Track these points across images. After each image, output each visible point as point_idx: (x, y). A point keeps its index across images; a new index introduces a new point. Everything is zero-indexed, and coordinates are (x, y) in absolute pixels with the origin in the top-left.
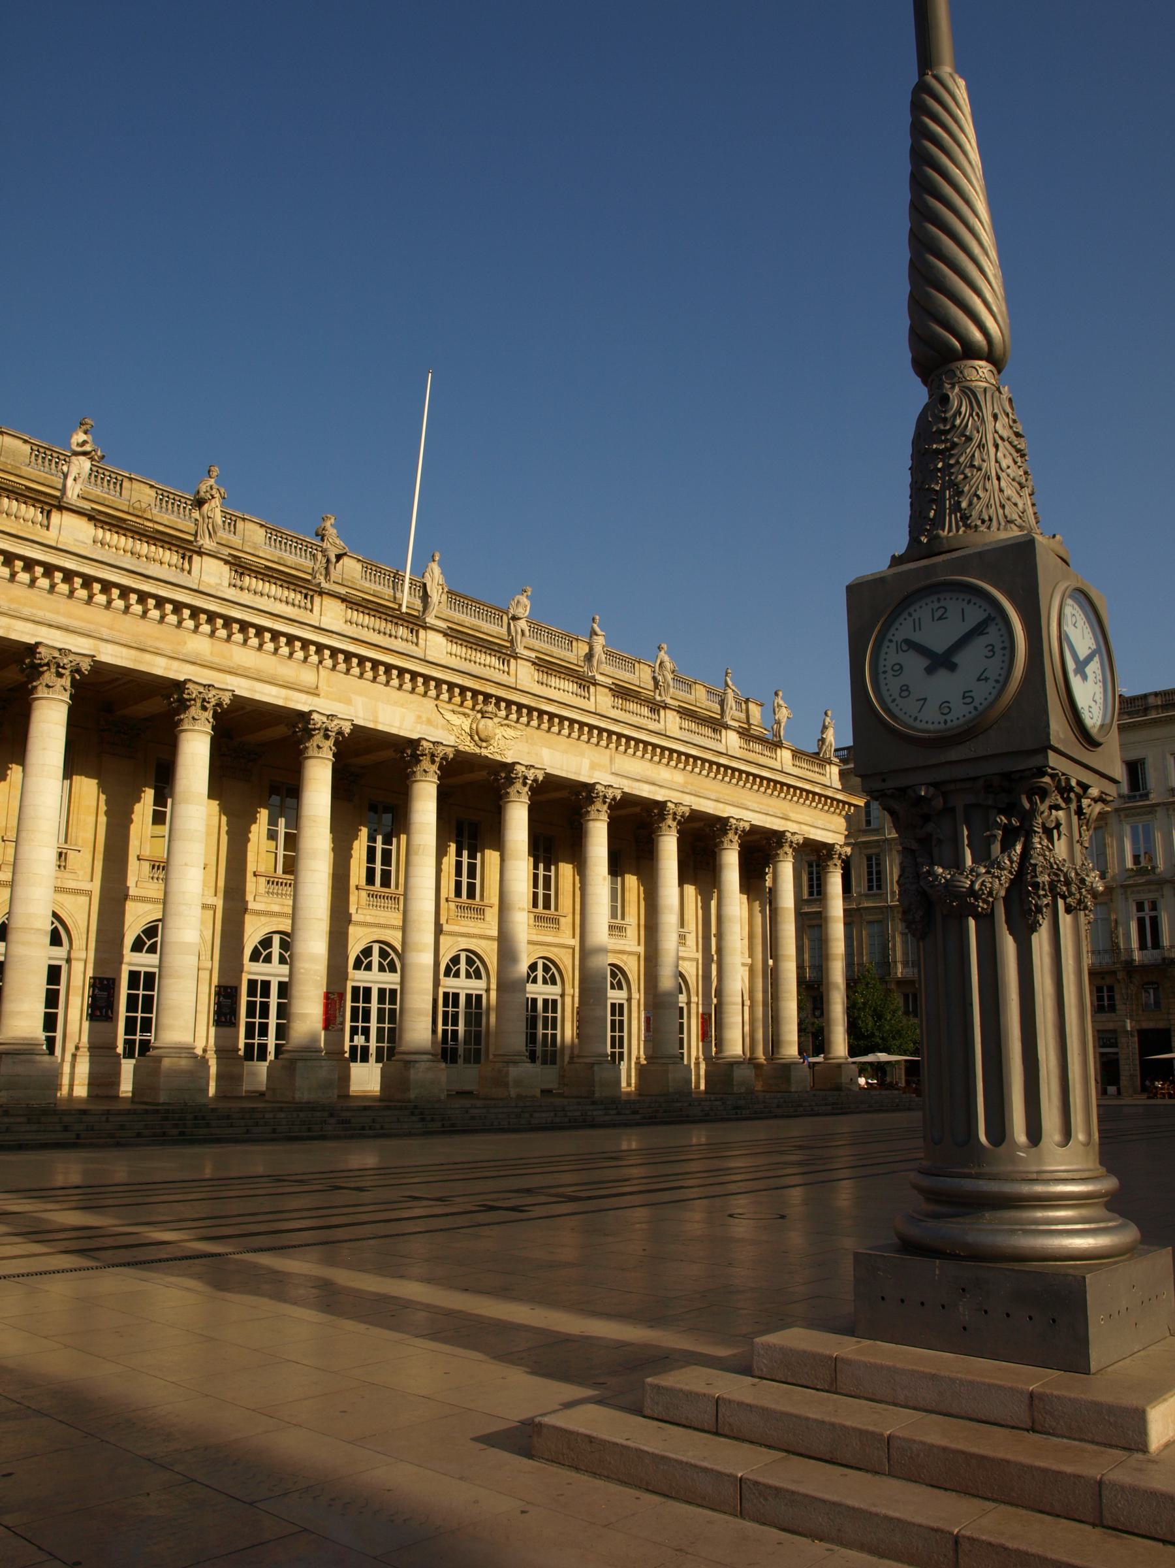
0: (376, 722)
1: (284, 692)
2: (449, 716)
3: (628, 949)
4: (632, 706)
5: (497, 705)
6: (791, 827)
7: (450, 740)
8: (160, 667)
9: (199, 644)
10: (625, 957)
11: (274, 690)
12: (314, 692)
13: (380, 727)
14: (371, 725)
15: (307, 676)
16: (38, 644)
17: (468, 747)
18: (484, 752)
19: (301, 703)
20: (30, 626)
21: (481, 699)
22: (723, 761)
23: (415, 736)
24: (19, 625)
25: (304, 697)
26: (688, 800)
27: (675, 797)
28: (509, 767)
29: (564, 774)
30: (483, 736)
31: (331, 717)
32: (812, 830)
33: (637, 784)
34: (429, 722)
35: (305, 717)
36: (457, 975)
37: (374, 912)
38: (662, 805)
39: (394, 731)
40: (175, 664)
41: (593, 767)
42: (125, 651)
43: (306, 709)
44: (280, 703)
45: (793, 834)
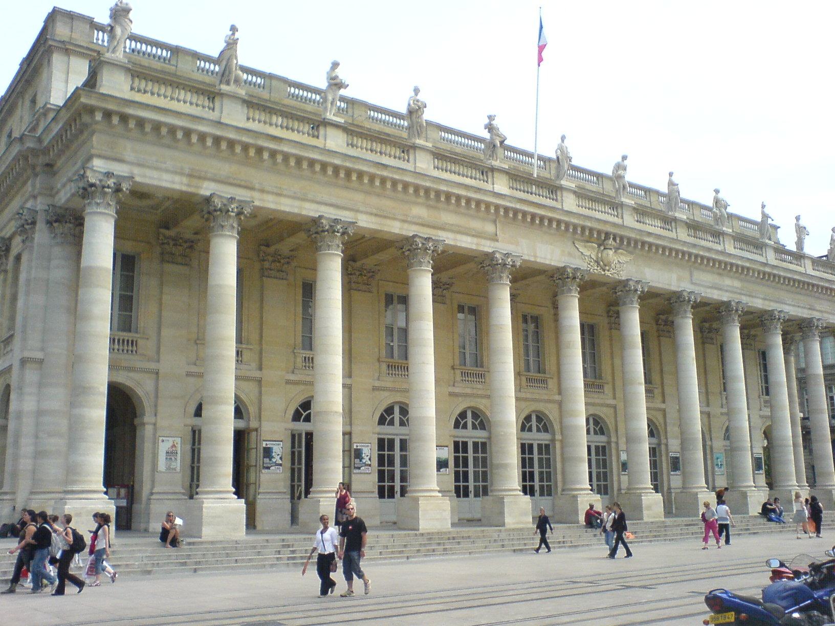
0: (535, 256)
1: (475, 240)
4: (700, 234)
5: (614, 239)
6: (817, 315)
7: (584, 266)
8: (396, 228)
9: (419, 211)
11: (469, 239)
12: (494, 238)
13: (538, 260)
14: (532, 259)
15: (490, 228)
16: (321, 217)
17: (596, 270)
18: (608, 273)
19: (487, 247)
20: (314, 206)
23: (561, 265)
24: (307, 205)
25: (488, 243)
26: (745, 299)
27: (735, 298)
28: (625, 284)
29: (660, 286)
30: (606, 262)
31: (507, 255)
34: (570, 254)
35: (490, 256)
38: (727, 304)
39: (547, 262)
40: (406, 226)
41: (679, 279)
42: (374, 219)
43: (490, 250)
44: (474, 247)
45: (818, 320)
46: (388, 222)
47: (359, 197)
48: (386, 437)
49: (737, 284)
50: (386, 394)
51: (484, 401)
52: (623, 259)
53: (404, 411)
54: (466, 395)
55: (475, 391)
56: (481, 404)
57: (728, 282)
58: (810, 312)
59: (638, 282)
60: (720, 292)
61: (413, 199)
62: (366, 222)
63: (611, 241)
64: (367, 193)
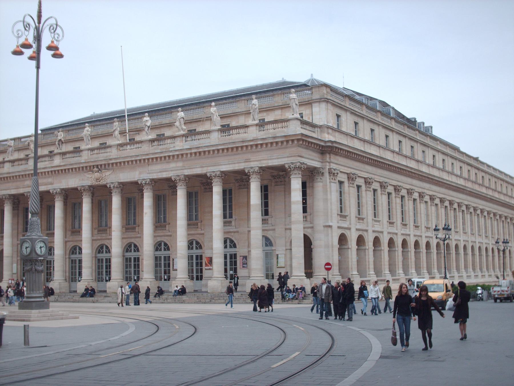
1: (46, 186)
2: (88, 176)
3: (232, 230)
7: (89, 183)
8: (21, 191)
10: (233, 234)
12: (52, 184)
14: (67, 187)
15: (50, 180)
17: (95, 183)
21: (89, 168)
22: (193, 151)
27: (179, 173)
32: (270, 161)
33: (160, 174)
34: (83, 180)
36: (131, 251)
37: (127, 233)
46: (19, 190)
47: (10, 184)
48: (199, 254)
49: (180, 164)
50: (72, 243)
51: (107, 241)
52: (108, 173)
53: (80, 249)
54: (99, 240)
55: (102, 238)
56: (106, 242)
57: (173, 165)
58: (247, 164)
59: (112, 183)
60: (167, 173)
61: (22, 179)
62: (13, 192)
63: (96, 169)
64: (13, 182)
